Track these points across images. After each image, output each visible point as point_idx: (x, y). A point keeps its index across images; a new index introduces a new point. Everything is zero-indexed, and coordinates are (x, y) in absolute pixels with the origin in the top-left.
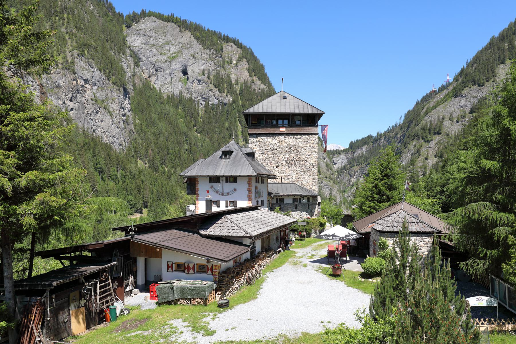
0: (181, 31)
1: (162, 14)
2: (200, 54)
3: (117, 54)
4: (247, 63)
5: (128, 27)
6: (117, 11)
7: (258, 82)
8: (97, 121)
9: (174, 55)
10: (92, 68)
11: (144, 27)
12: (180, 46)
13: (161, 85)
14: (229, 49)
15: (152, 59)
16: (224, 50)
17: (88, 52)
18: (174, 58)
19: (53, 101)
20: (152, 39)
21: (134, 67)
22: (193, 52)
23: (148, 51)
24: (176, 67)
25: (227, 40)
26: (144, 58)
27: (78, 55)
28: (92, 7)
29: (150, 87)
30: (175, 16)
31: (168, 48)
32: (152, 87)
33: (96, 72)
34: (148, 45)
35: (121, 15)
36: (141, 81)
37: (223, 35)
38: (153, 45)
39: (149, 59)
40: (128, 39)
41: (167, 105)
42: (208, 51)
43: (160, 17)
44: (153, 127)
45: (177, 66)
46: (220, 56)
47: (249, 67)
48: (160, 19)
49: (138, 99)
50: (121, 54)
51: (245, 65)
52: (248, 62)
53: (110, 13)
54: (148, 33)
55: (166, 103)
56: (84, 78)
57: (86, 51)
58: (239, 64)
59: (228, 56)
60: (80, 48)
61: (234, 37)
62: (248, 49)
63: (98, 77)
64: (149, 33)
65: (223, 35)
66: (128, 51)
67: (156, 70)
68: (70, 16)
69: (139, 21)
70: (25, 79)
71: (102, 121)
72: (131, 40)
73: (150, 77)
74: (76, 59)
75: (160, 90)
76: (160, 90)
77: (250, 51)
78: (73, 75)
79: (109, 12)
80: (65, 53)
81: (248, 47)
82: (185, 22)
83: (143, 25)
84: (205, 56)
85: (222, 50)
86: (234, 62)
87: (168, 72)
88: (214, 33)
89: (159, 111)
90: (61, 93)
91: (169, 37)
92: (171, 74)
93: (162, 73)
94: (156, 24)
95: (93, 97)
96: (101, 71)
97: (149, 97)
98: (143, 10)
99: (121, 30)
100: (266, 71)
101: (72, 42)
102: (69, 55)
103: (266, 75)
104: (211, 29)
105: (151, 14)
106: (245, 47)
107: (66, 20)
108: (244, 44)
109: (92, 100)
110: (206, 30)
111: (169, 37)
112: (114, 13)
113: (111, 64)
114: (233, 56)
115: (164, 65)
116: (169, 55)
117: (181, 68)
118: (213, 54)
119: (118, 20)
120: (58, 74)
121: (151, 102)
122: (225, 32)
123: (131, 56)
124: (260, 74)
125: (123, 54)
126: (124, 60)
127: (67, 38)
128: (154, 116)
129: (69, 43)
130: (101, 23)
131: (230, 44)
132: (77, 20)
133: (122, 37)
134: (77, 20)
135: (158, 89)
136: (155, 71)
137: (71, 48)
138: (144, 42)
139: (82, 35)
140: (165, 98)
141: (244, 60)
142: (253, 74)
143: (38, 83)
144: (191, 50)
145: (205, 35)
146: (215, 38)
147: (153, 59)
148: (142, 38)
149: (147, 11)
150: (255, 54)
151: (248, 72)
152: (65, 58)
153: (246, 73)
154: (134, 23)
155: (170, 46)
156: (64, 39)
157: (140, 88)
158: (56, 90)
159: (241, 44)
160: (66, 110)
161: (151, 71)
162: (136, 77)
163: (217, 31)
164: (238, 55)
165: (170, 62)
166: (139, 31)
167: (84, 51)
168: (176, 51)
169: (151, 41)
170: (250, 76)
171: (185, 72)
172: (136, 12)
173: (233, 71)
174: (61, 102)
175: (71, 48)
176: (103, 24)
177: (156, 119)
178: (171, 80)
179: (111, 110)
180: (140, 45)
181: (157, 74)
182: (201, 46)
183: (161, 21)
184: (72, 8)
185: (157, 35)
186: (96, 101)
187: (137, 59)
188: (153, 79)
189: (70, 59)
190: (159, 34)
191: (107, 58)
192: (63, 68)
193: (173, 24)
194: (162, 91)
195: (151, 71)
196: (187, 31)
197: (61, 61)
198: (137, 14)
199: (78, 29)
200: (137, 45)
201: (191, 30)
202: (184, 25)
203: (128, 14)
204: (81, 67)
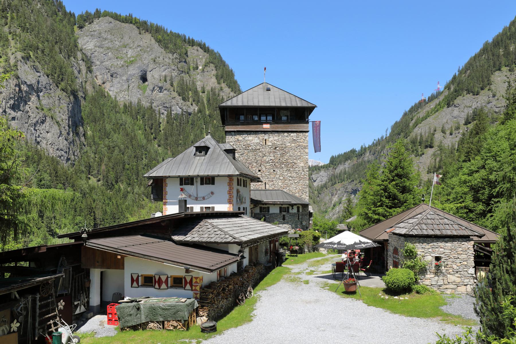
0: (140, 34)
1: (119, 14)
2: (161, 58)
3: (67, 58)
4: (214, 69)
5: (81, 27)
6: (68, 11)
7: (227, 90)
9: (131, 59)
11: (98, 28)
12: (139, 49)
13: (117, 93)
14: (193, 52)
15: (107, 63)
16: (189, 54)
17: (34, 55)
18: (132, 62)
20: (106, 42)
21: (87, 73)
22: (153, 56)
23: (102, 55)
24: (134, 72)
25: (192, 43)
26: (98, 63)
27: (23, 58)
28: (39, 5)
29: (104, 95)
30: (134, 17)
31: (125, 52)
32: (106, 95)
33: (42, 76)
34: (102, 48)
35: (72, 15)
36: (94, 88)
37: (187, 38)
38: (108, 48)
39: (104, 64)
40: (79, 41)
41: (123, 115)
42: (170, 55)
43: (116, 17)
44: (107, 139)
45: (134, 71)
46: (184, 60)
47: (217, 73)
48: (117, 20)
49: (91, 108)
50: (72, 58)
51: (212, 71)
52: (216, 67)
53: (60, 13)
54: (103, 35)
55: (122, 111)
56: (29, 83)
57: (31, 53)
58: (205, 70)
59: (193, 60)
60: (25, 50)
61: (200, 40)
62: (215, 53)
63: (44, 83)
64: (104, 35)
65: (187, 38)
66: (79, 55)
67: (112, 76)
68: (14, 14)
69: (93, 22)
71: (48, 132)
72: (83, 42)
73: (104, 83)
74: (19, 62)
75: (116, 98)
76: (116, 98)
77: (217, 55)
78: (15, 80)
79: (59, 11)
81: (216, 51)
82: (145, 23)
83: (97, 26)
84: (167, 60)
85: (186, 53)
86: (200, 68)
87: (124, 78)
88: (178, 36)
89: (114, 121)
91: (126, 40)
92: (128, 80)
93: (118, 79)
94: (112, 25)
96: (48, 76)
97: (103, 105)
98: (97, 10)
99: (73, 31)
100: (236, 78)
101: (16, 43)
102: (12, 58)
103: (235, 82)
104: (174, 31)
105: (106, 14)
106: (213, 51)
107: (9, 18)
108: (211, 48)
109: (37, 108)
110: (169, 32)
111: (126, 40)
112: (65, 13)
113: (61, 68)
114: (198, 61)
115: (120, 70)
116: (126, 59)
117: (140, 74)
118: (176, 58)
119: (69, 20)
121: (105, 111)
122: (190, 34)
123: (83, 61)
124: (229, 81)
125: (74, 58)
126: (75, 64)
128: (108, 127)
129: (12, 43)
130: (49, 23)
131: (195, 47)
132: (22, 19)
133: (73, 39)
134: (22, 19)
135: (113, 97)
136: (110, 77)
137: (14, 50)
138: (98, 44)
139: (28, 37)
140: (122, 107)
141: (211, 65)
142: (222, 81)
144: (152, 54)
145: (168, 38)
146: (179, 41)
147: (108, 63)
148: (96, 40)
149: (102, 11)
150: (224, 58)
151: (216, 79)
152: (6, 61)
153: (214, 80)
154: (87, 24)
156: (7, 40)
157: (93, 96)
159: (208, 48)
162: (88, 83)
163: (181, 33)
164: (204, 60)
165: (127, 66)
166: (92, 33)
167: (29, 53)
168: (134, 54)
169: (106, 44)
170: (219, 83)
171: (144, 79)
172: (89, 11)
173: (199, 77)
175: (14, 50)
176: (52, 25)
177: (111, 130)
178: (129, 87)
179: (59, 119)
181: (112, 81)
182: (163, 50)
183: (118, 22)
184: (16, 6)
185: (113, 37)
186: (43, 109)
188: (107, 86)
189: (12, 62)
190: (115, 36)
191: (55, 61)
193: (131, 25)
194: (118, 99)
196: (147, 33)
198: (90, 14)
199: (24, 29)
200: (90, 48)
201: (152, 32)
202: (144, 27)
203: (80, 13)
204: (25, 71)
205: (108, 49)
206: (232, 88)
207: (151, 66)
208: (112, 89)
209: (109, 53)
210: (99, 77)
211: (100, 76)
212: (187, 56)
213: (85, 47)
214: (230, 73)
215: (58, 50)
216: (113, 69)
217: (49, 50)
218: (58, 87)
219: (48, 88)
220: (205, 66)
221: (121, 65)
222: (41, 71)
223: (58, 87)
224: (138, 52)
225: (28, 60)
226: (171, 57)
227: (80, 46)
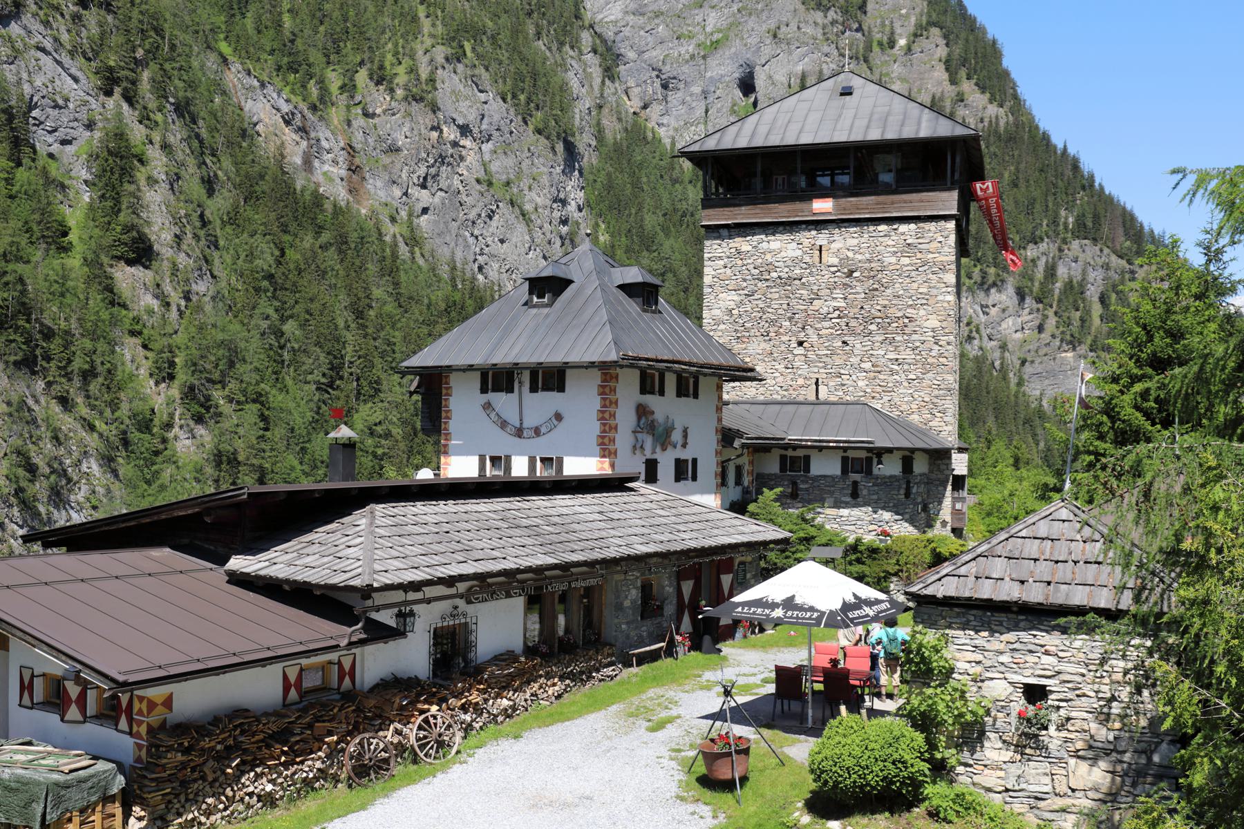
2: (793, 26)
3: (554, 48)
4: (942, 42)
7: (977, 99)
8: (489, 240)
9: (716, 36)
10: (481, 91)
13: (676, 130)
15: (654, 53)
17: (473, 49)
18: (716, 45)
19: (378, 191)
21: (603, 83)
23: (642, 33)
24: (722, 71)
26: (631, 55)
27: (447, 59)
31: (699, 19)
32: (650, 135)
33: (492, 101)
34: (643, 14)
36: (620, 120)
39: (646, 56)
41: (690, 187)
42: (818, 16)
44: (645, 253)
45: (724, 69)
46: (855, 26)
47: (949, 55)
49: (609, 175)
51: (935, 47)
52: (945, 37)
56: (460, 122)
57: (468, 47)
58: (916, 48)
59: (883, 25)
60: (453, 39)
63: (496, 117)
66: (586, 38)
67: (665, 86)
70: (313, 135)
71: (502, 241)
73: (645, 107)
74: (440, 71)
80: (412, 57)
84: (809, 30)
86: (902, 42)
87: (696, 89)
89: (666, 204)
90: (398, 166)
92: (705, 94)
93: (680, 94)
95: (481, 175)
96: (504, 100)
97: (640, 166)
100: (1007, 62)
101: (434, 25)
102: (423, 60)
109: (478, 181)
113: (535, 76)
114: (897, 25)
115: (685, 69)
116: (702, 38)
117: (737, 75)
118: (834, 22)
120: (394, 114)
121: (644, 179)
123: (595, 51)
124: (985, 73)
125: (572, 47)
126: (574, 63)
127: (422, 14)
128: (651, 221)
129: (426, 24)
135: (667, 141)
136: (659, 90)
137: (429, 42)
141: (935, 31)
142: (963, 73)
143: (342, 144)
147: (656, 55)
151: (947, 69)
152: (412, 70)
153: (941, 74)
155: (706, 9)
156: (415, 19)
157: (615, 143)
158: (386, 159)
160: (410, 215)
161: (650, 90)
162: (606, 111)
164: (913, 19)
165: (704, 57)
167: (462, 47)
168: (723, 23)
170: (953, 81)
171: (747, 86)
173: (896, 69)
174: (397, 192)
175: (429, 42)
177: (658, 229)
178: (707, 111)
179: (528, 207)
180: (620, 16)
181: (665, 98)
186: (490, 184)
187: (610, 59)
188: (655, 111)
192: (406, 99)
195: (650, 90)
197: (402, 79)
200: (612, 18)
205: (657, 16)
206: (992, 95)
207: (767, 51)
208: (665, 122)
209: (658, 25)
210: (635, 91)
211: (637, 90)
212: (865, 13)
213: (601, 16)
214: (989, 49)
215: (531, 30)
216: (668, 68)
217: (508, 33)
218: (526, 123)
219: (506, 130)
220: (915, 35)
221: (687, 57)
222: (488, 88)
223: (526, 123)
224: (734, 15)
225: (459, 61)
226: (820, 21)
227: (588, 16)
